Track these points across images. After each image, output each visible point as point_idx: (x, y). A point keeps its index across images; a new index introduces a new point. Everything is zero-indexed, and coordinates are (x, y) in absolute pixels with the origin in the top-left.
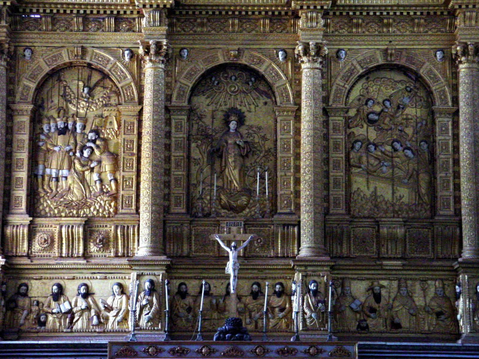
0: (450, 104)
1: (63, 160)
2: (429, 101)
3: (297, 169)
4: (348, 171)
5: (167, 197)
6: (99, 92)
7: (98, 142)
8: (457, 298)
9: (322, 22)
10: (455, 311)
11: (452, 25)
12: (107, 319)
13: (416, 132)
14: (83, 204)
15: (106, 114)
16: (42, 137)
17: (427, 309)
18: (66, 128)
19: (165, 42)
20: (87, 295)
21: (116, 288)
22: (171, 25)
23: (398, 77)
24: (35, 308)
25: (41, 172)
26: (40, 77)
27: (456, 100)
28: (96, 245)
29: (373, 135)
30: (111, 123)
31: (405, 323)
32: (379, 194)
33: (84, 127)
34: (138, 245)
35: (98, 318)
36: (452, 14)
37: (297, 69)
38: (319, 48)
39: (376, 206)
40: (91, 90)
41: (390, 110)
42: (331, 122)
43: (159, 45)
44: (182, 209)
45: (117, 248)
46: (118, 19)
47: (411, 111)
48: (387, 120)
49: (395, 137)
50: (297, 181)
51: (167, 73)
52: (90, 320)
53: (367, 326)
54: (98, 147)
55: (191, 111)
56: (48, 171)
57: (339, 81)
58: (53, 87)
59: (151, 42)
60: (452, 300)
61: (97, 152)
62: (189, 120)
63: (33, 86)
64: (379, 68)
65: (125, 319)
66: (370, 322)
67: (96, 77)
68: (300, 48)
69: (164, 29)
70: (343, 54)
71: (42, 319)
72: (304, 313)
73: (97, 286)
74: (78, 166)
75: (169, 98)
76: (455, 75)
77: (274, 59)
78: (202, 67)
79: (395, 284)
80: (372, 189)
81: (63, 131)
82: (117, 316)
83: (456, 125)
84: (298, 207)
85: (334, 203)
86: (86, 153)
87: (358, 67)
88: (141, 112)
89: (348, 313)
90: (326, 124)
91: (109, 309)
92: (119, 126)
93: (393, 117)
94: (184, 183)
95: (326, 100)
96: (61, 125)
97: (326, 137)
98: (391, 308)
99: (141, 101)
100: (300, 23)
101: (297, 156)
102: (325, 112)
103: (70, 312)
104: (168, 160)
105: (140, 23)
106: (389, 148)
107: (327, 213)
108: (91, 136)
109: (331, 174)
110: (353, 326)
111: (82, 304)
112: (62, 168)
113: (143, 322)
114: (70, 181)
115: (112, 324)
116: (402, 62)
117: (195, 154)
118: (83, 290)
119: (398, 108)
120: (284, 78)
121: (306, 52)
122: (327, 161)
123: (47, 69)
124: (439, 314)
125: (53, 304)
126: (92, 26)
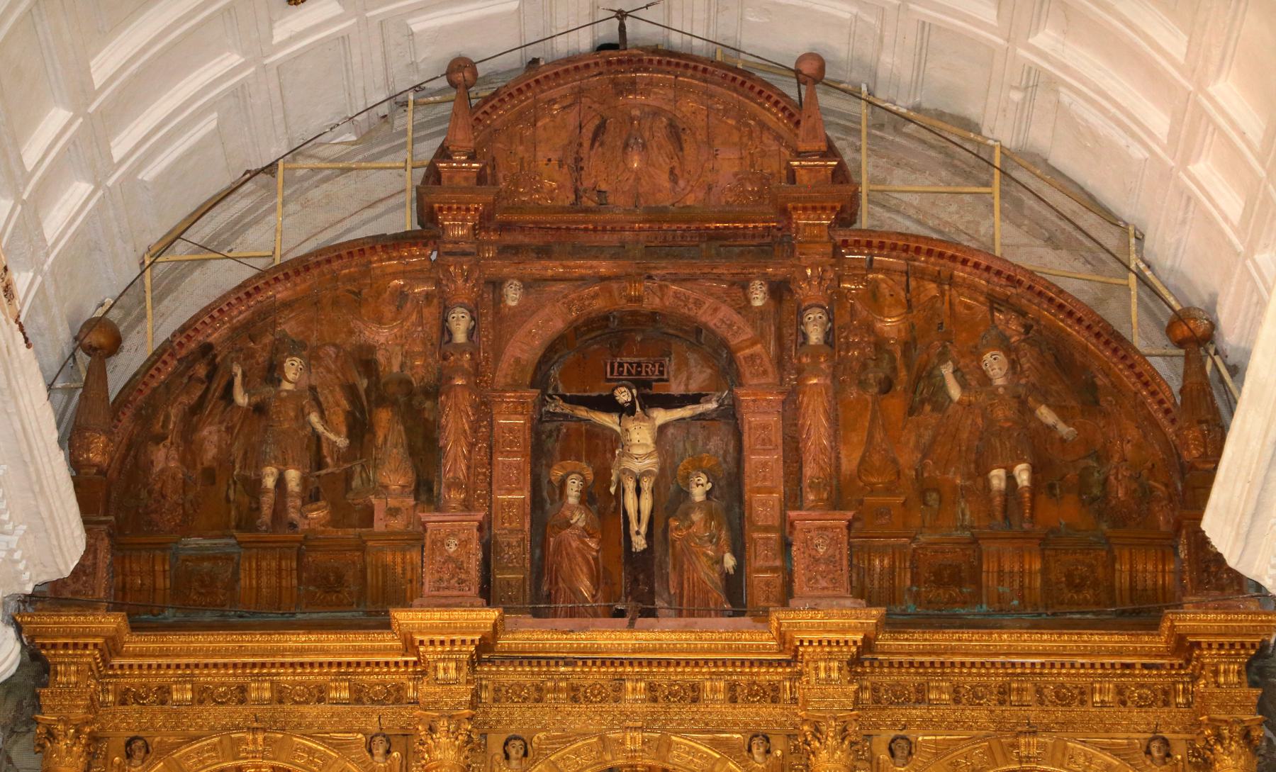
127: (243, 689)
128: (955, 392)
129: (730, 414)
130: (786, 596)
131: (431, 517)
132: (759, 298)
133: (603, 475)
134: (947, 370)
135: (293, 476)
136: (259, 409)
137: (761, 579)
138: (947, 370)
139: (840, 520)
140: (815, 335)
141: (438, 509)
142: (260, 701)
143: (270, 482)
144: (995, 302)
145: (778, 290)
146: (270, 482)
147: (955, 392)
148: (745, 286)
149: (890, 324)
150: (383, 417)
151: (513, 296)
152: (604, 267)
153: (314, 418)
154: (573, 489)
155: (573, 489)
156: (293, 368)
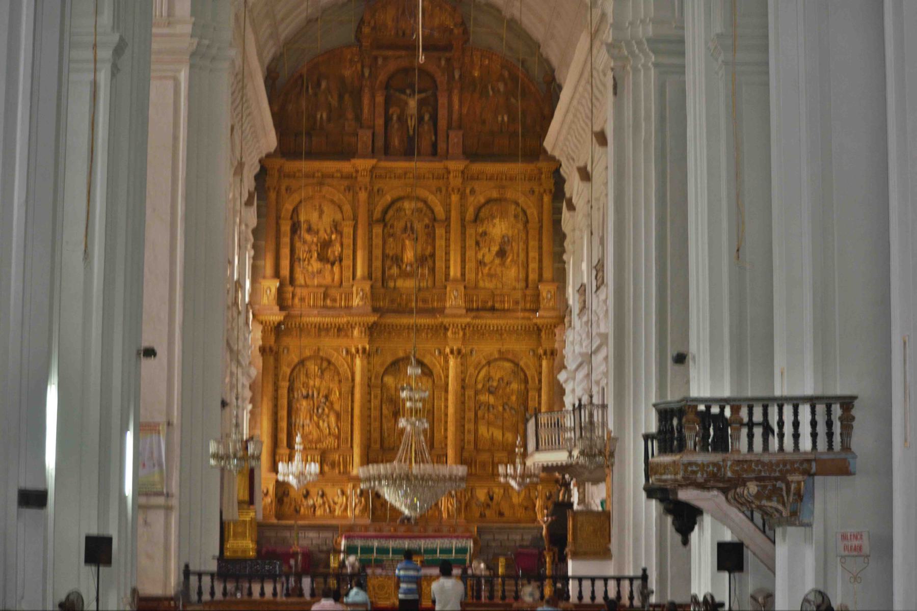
0: (537, 382)
1: (306, 415)
2: (526, 381)
3: (446, 422)
4: (476, 422)
5: (369, 439)
6: (327, 376)
7: (327, 403)
8: (536, 499)
9: (461, 333)
10: (535, 506)
11: (539, 335)
12: (335, 511)
13: (517, 398)
14: (319, 441)
15: (331, 386)
16: (295, 401)
17: (520, 505)
18: (308, 395)
19: (367, 347)
20: (323, 495)
21: (339, 492)
22: (371, 335)
23: (508, 365)
24: (293, 503)
25: (293, 421)
26: (292, 366)
27: (540, 381)
28: (327, 465)
29: (492, 400)
30: (335, 392)
31: (507, 512)
32: (494, 438)
33: (319, 394)
34: (352, 469)
35: (330, 507)
36: (539, 330)
37: (447, 361)
38: (459, 352)
39: (493, 444)
40: (322, 373)
41: (503, 385)
42: (466, 393)
43: (364, 349)
44: (378, 446)
45: (340, 468)
46: (339, 330)
47: (515, 386)
48: (501, 391)
49: (505, 401)
50: (446, 430)
51: (369, 363)
52: (325, 510)
53: (485, 516)
54: (328, 407)
55: (383, 386)
56: (298, 421)
57: (471, 370)
58: (300, 370)
59: (360, 347)
60: (534, 499)
61: (326, 410)
62: (381, 390)
63: (288, 371)
64: (496, 360)
65: (346, 509)
66: (488, 512)
67: (325, 364)
68: (448, 350)
69: (367, 339)
70: (474, 353)
71: (298, 509)
72: (448, 508)
73: (329, 491)
74: (315, 418)
75: (370, 379)
76: (541, 366)
77: (433, 355)
78: (389, 360)
79: (502, 491)
80: (490, 433)
81: (307, 397)
82: (341, 507)
83: (540, 396)
84: (446, 445)
85: (468, 442)
86: (320, 411)
87: (483, 360)
88: (353, 387)
89: (474, 506)
90: (463, 395)
91: (335, 503)
92: (340, 394)
93: (505, 388)
94: (378, 430)
95: (463, 380)
96: (305, 393)
97: (463, 403)
98: (498, 504)
99: (353, 380)
100: (449, 333)
101: (446, 415)
102: (463, 388)
103: (314, 506)
104: (370, 416)
105: (352, 333)
106: (501, 409)
107: (463, 448)
108: (323, 400)
109: (466, 427)
110: (478, 515)
111: (320, 501)
112: (306, 418)
113: (357, 512)
114: (311, 427)
115: (338, 512)
116: (510, 357)
117: (385, 411)
118: (320, 493)
119: (507, 383)
120: (438, 366)
121: (452, 352)
122: (464, 418)
123: (296, 360)
124: (526, 508)
125: (303, 500)
126: (323, 333)
127: (314, 174)
128: (491, 93)
129: (435, 97)
130: (446, 156)
131: (360, 132)
132: (443, 62)
133: (403, 111)
134: (490, 87)
135: (324, 116)
136: (316, 94)
137: (442, 146)
138: (490, 87)
139: (460, 133)
140: (457, 76)
141: (361, 127)
142: (318, 177)
143: (319, 116)
144: (503, 67)
145: (448, 60)
146: (319, 116)
147: (491, 93)
148: (440, 59)
149: (476, 75)
150: (347, 97)
151: (380, 61)
152: (403, 53)
153: (329, 97)
154: (395, 118)
155: (395, 118)
156: (324, 84)
